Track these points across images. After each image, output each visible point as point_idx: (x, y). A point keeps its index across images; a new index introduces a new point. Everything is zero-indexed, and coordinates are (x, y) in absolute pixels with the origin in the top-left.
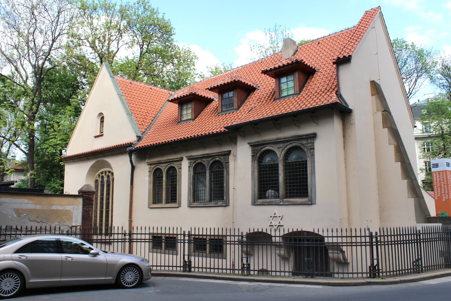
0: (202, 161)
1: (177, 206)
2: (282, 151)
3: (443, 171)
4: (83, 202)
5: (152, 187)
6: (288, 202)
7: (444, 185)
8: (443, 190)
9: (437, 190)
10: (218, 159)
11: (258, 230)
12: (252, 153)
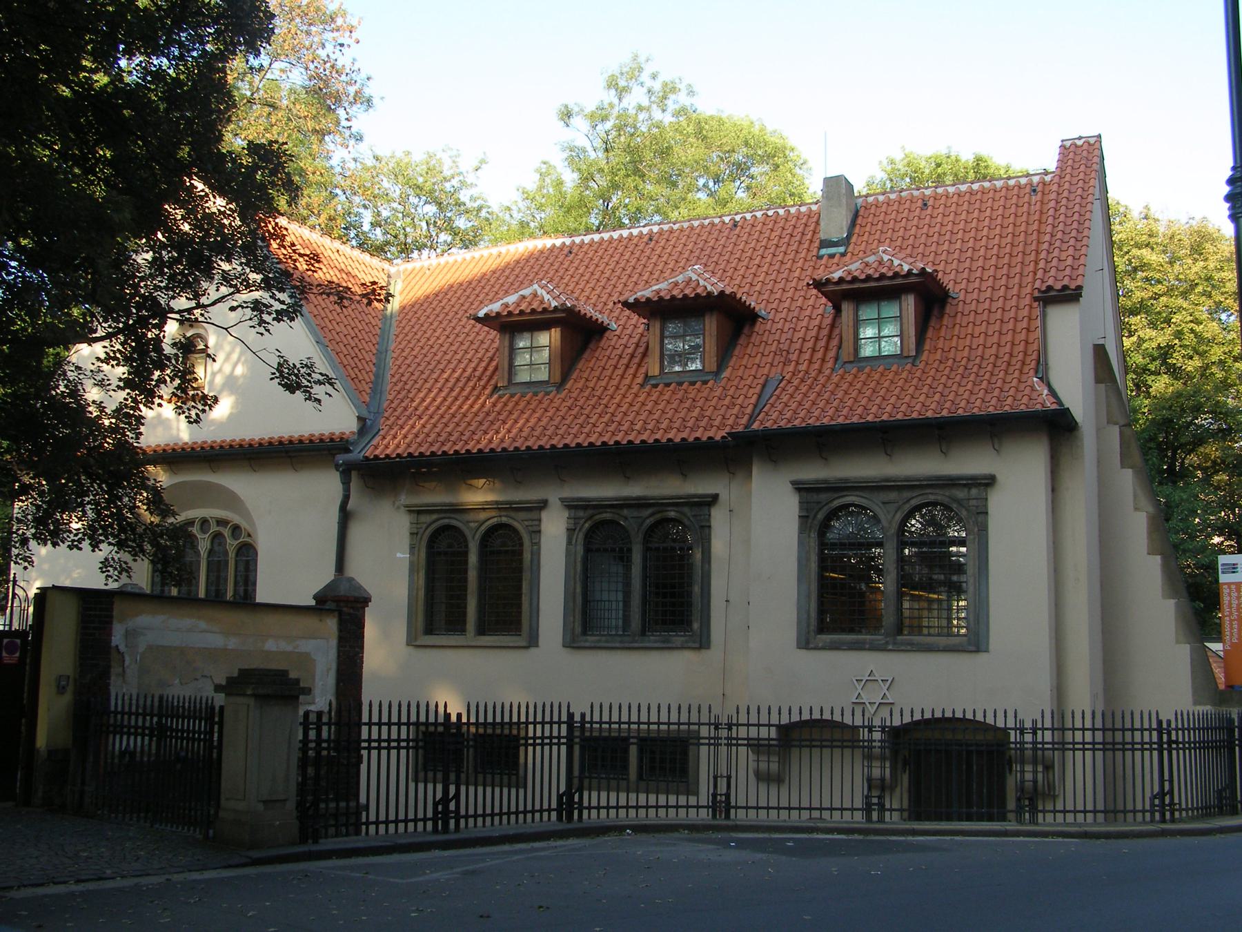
0: (616, 517)
1: (524, 644)
4: (340, 631)
5: (422, 582)
9: (1231, 628)
10: (672, 514)
11: (954, 712)
12: (801, 509)
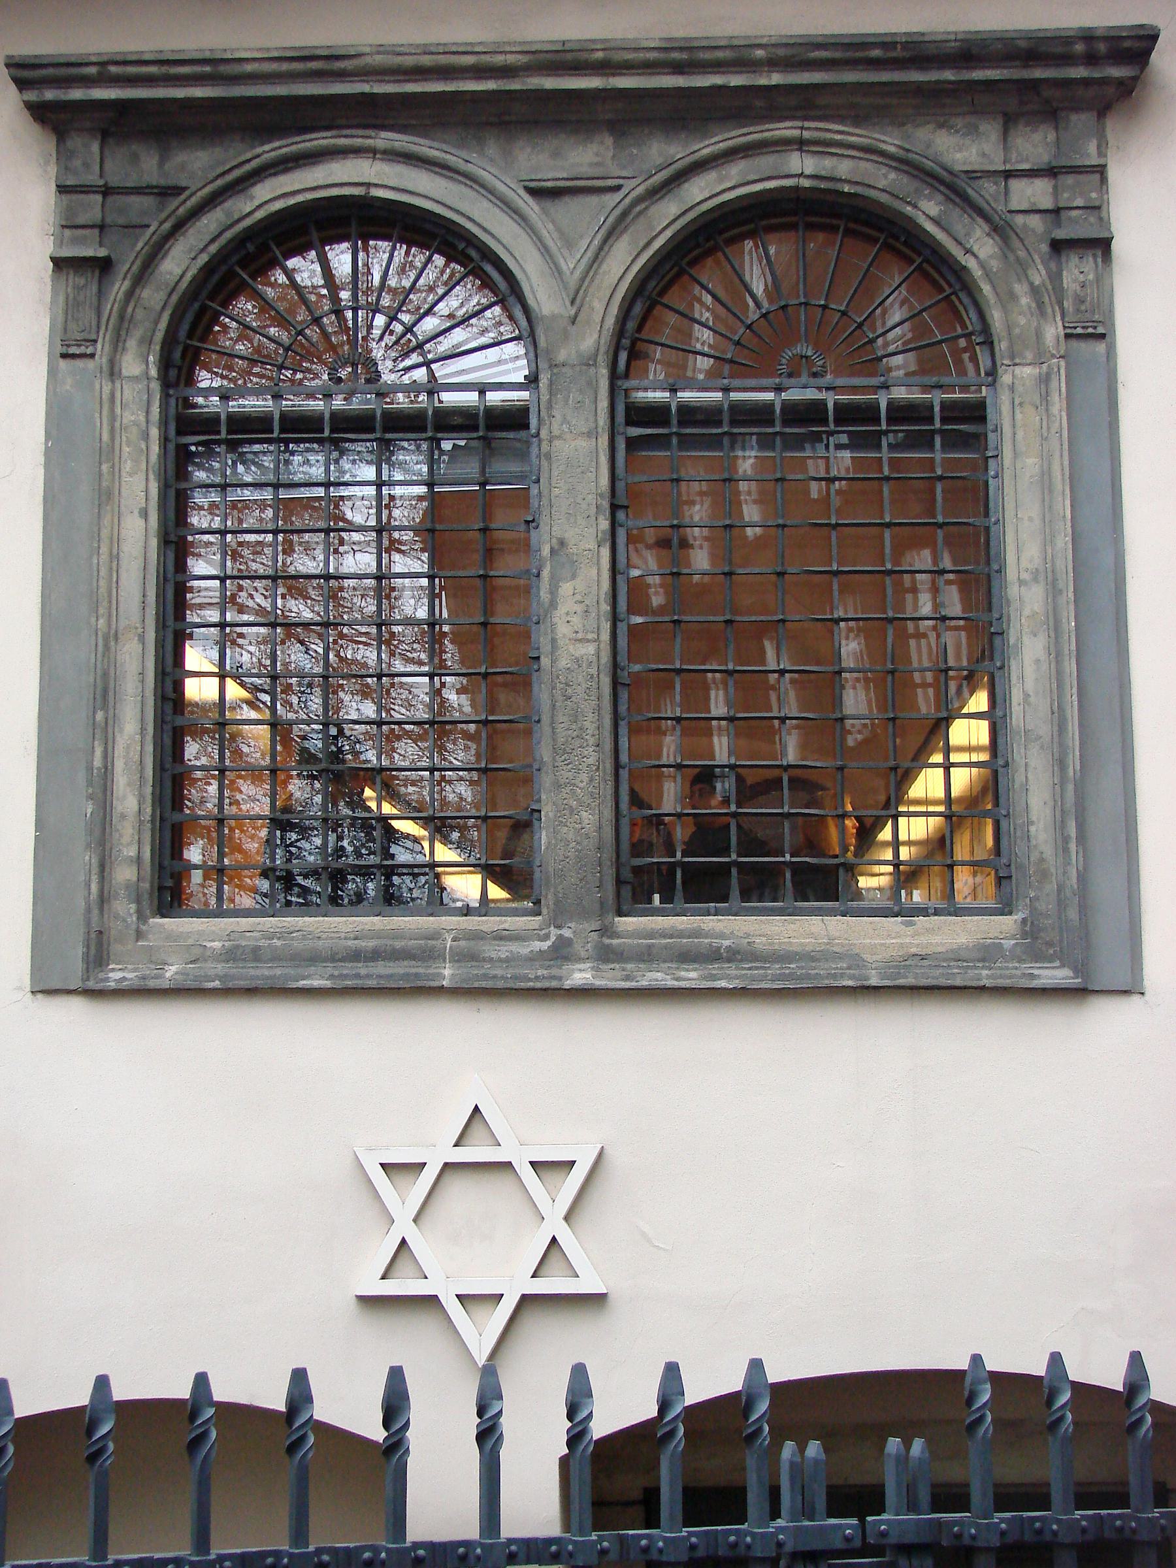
2: (612, 234)
6: (686, 957)
12: (69, 225)
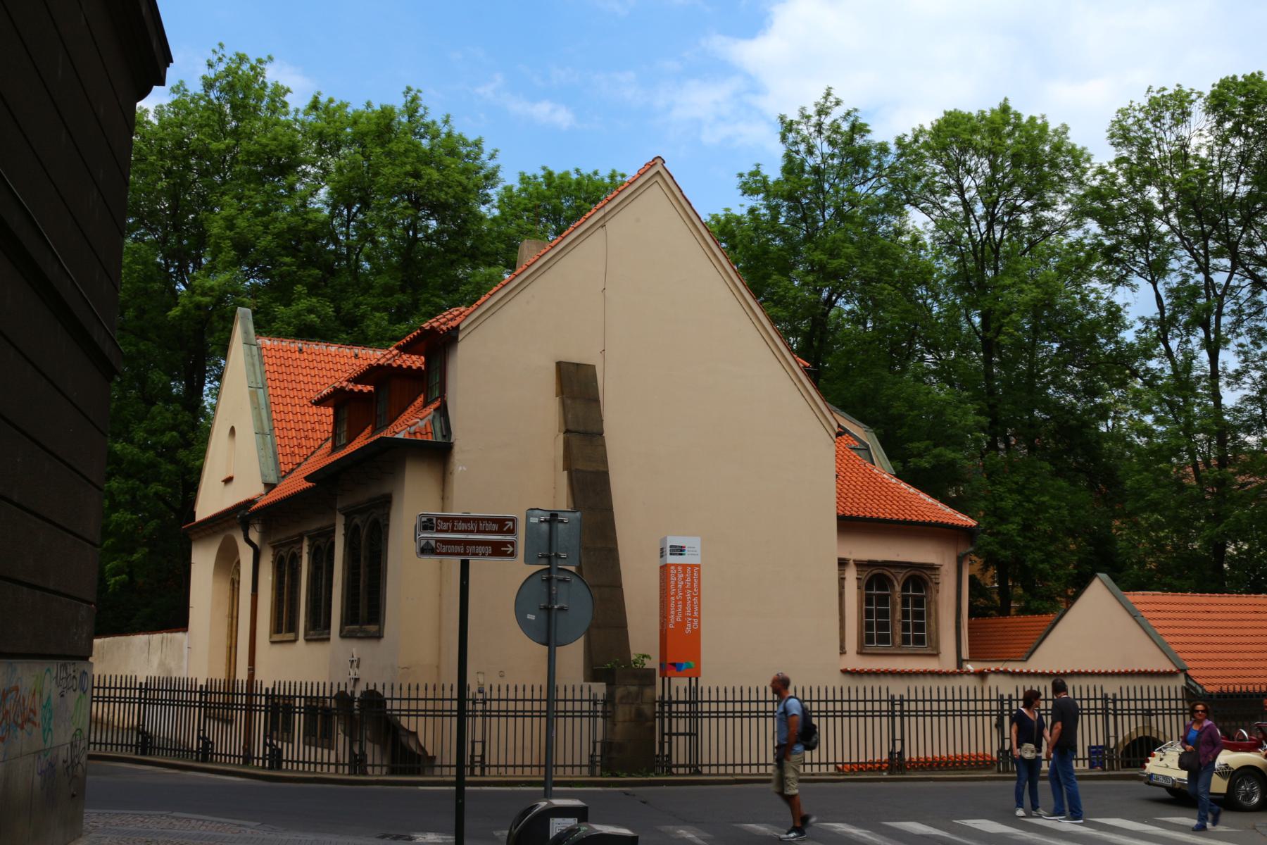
3: (692, 566)
7: (692, 597)
8: (688, 608)
9: (676, 608)
